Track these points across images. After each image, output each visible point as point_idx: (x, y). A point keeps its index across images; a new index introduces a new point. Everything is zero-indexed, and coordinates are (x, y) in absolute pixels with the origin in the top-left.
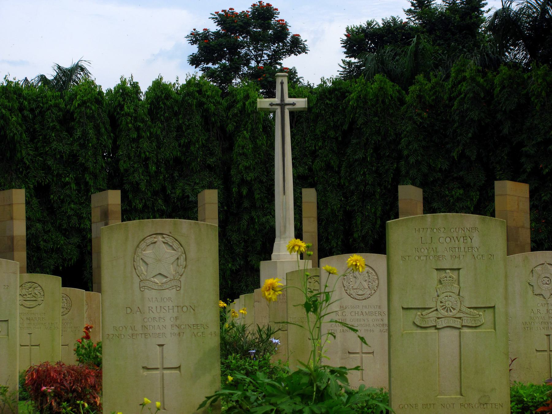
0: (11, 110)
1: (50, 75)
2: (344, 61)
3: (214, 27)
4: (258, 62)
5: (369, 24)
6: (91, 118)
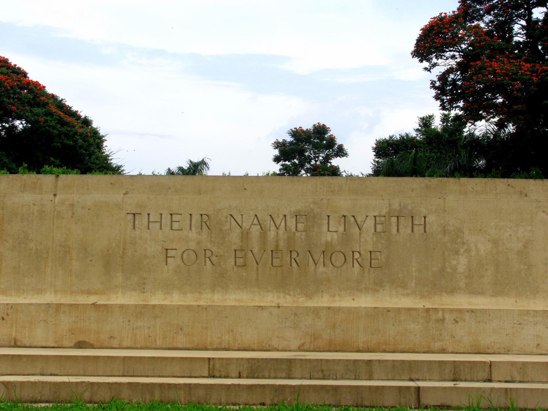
2: (374, 161)
3: (289, 139)
4: (316, 161)
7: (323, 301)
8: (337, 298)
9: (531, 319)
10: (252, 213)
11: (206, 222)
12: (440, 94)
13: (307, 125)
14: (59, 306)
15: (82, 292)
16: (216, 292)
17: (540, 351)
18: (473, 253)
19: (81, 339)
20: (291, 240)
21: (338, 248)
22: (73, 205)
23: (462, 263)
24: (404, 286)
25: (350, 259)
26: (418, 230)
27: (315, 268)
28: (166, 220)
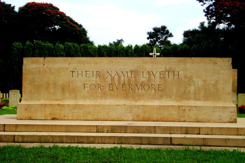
0: (105, 51)
1: (116, 41)
3: (153, 31)
4: (162, 39)
5: (189, 30)
6: (122, 53)
7: (141, 103)
8: (146, 101)
9: (217, 110)
10: (115, 71)
11: (98, 74)
12: (206, 14)
13: (159, 26)
14: (46, 105)
15: (54, 100)
16: (102, 99)
17: (221, 122)
18: (197, 85)
19: (54, 117)
20: (129, 80)
21: (147, 83)
22: (50, 68)
23: (192, 89)
24: (171, 97)
25: (151, 87)
26: (176, 77)
27: (138, 91)
28: (84, 73)
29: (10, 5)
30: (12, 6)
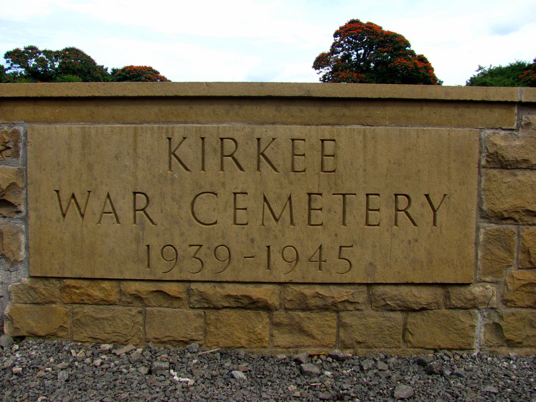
29: (103, 66)
30: (105, 68)
